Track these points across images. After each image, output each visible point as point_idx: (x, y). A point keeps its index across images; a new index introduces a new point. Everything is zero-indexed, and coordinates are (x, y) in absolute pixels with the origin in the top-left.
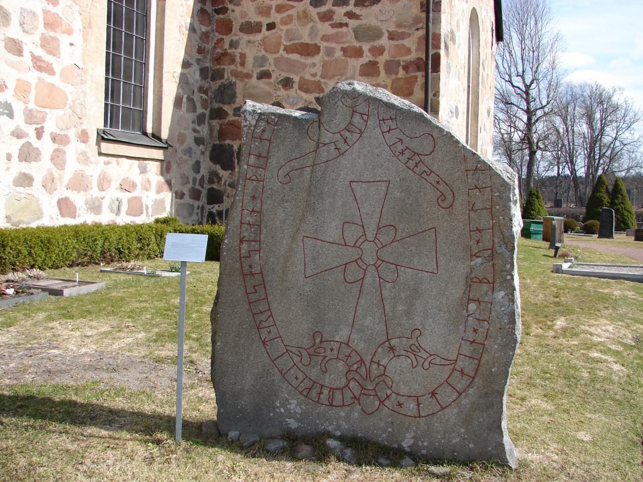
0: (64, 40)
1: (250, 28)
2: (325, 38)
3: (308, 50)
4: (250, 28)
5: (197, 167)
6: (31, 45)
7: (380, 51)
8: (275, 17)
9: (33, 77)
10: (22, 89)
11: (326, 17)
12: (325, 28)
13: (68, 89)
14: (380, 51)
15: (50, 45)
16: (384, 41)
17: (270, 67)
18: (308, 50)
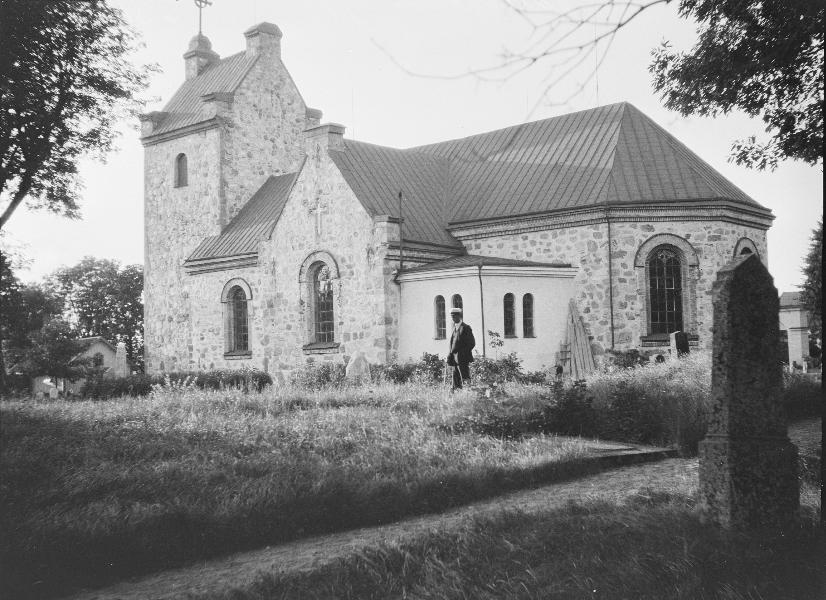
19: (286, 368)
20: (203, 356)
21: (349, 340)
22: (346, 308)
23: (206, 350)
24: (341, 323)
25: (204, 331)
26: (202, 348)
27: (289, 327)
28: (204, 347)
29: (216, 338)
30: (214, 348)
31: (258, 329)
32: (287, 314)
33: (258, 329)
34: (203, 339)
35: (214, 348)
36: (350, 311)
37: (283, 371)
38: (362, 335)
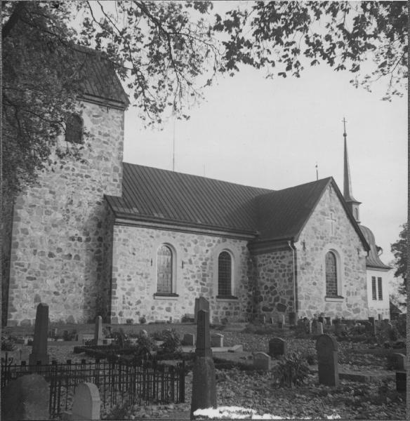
0: (207, 278)
1: (260, 266)
2: (275, 268)
3: (272, 271)
4: (260, 266)
5: (249, 303)
6: (200, 281)
7: (285, 270)
8: (265, 262)
9: (200, 287)
10: (198, 289)
11: (275, 262)
12: (275, 265)
13: (209, 288)
14: (285, 270)
15: (204, 280)
16: (286, 268)
17: (264, 276)
18: (272, 271)
19: (314, 308)
20: (129, 294)
21: (350, 295)
22: (349, 278)
23: (133, 290)
24: (345, 286)
25: (132, 273)
26: (128, 287)
27: (315, 284)
28: (129, 287)
29: (144, 280)
30: (141, 289)
31: (186, 278)
32: (313, 275)
33: (186, 278)
34: (130, 280)
35: (141, 289)
36: (350, 280)
37: (312, 310)
38: (356, 293)
